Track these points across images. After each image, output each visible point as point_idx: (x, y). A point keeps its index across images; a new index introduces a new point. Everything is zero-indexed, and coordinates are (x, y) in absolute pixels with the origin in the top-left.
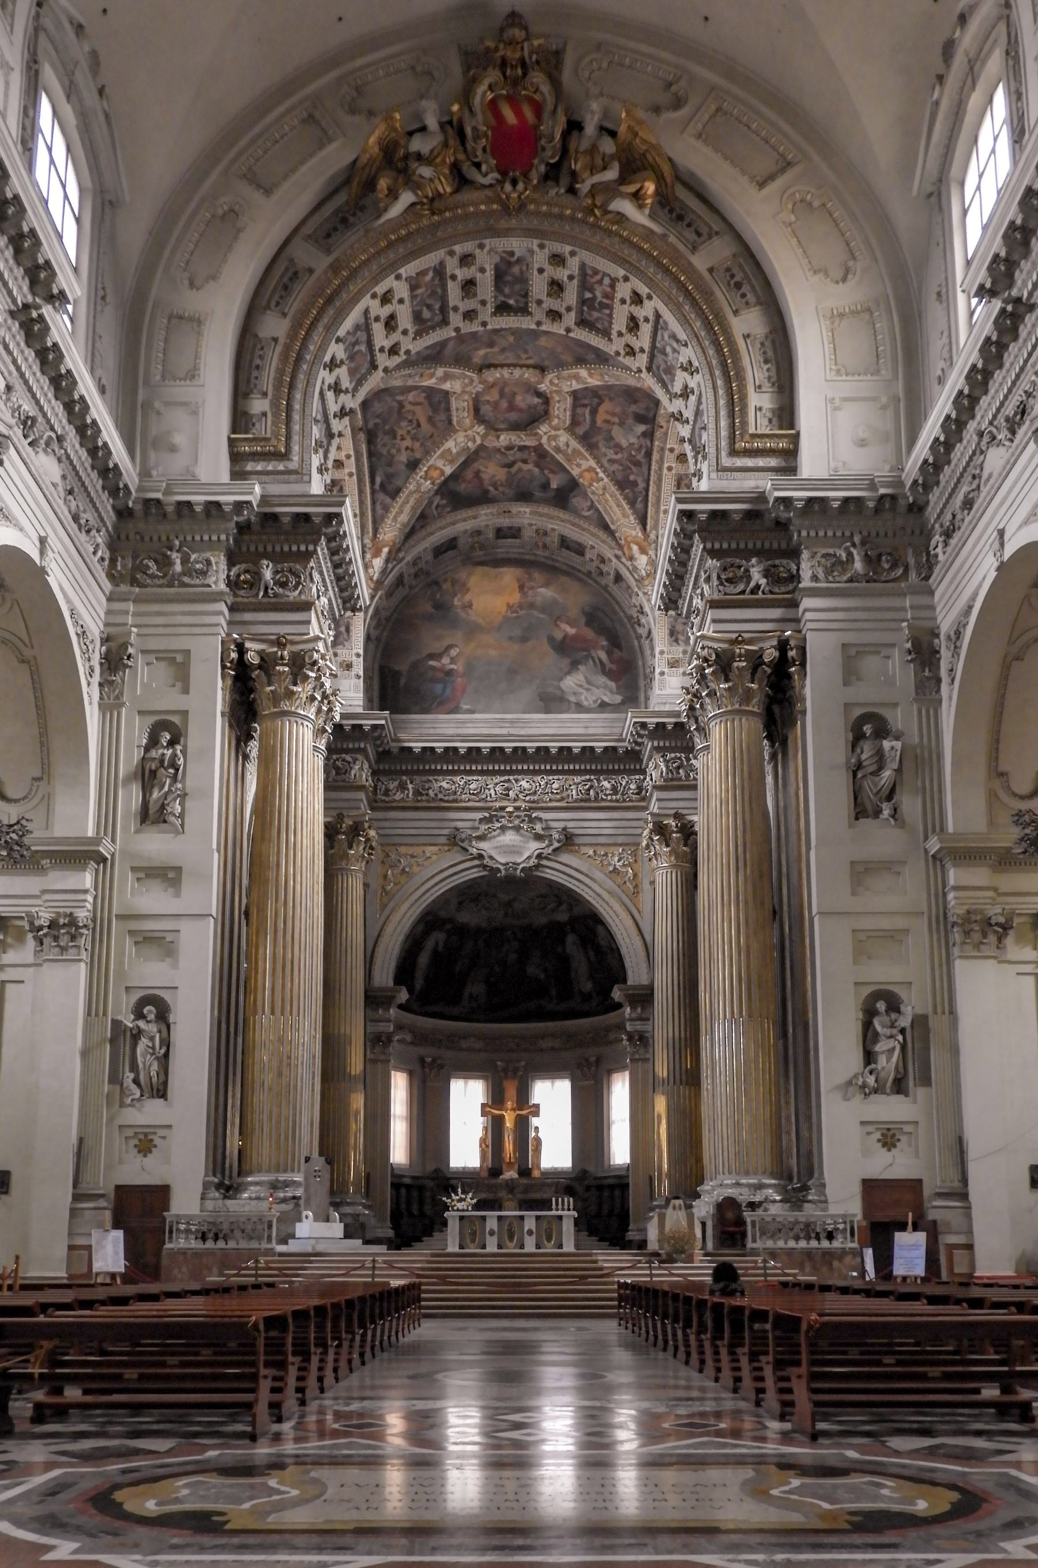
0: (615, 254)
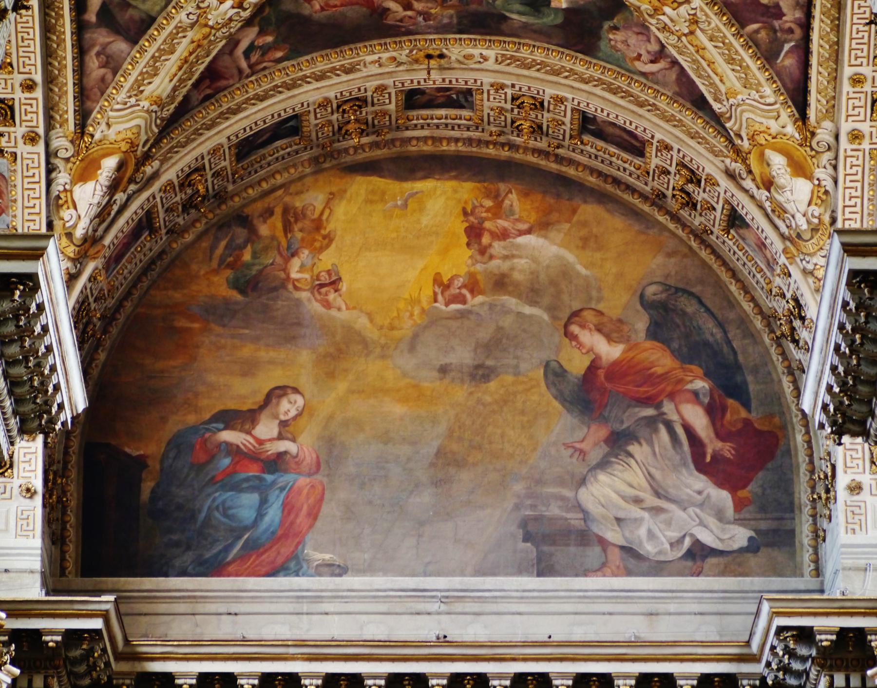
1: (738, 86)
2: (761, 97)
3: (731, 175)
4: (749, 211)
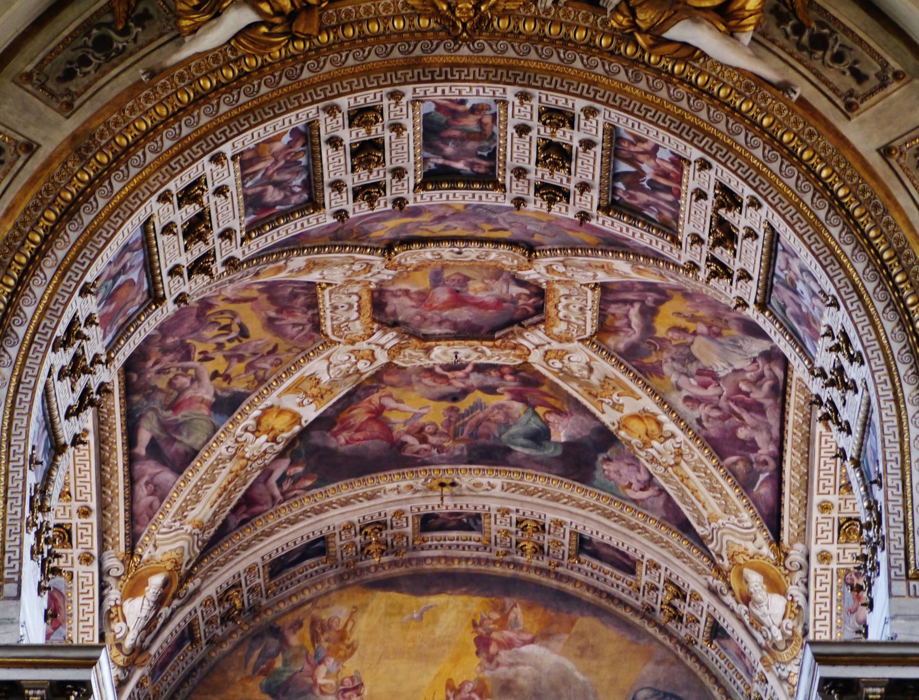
0: (682, 118)
1: (719, 511)
2: (740, 521)
3: (713, 591)
4: (730, 623)
